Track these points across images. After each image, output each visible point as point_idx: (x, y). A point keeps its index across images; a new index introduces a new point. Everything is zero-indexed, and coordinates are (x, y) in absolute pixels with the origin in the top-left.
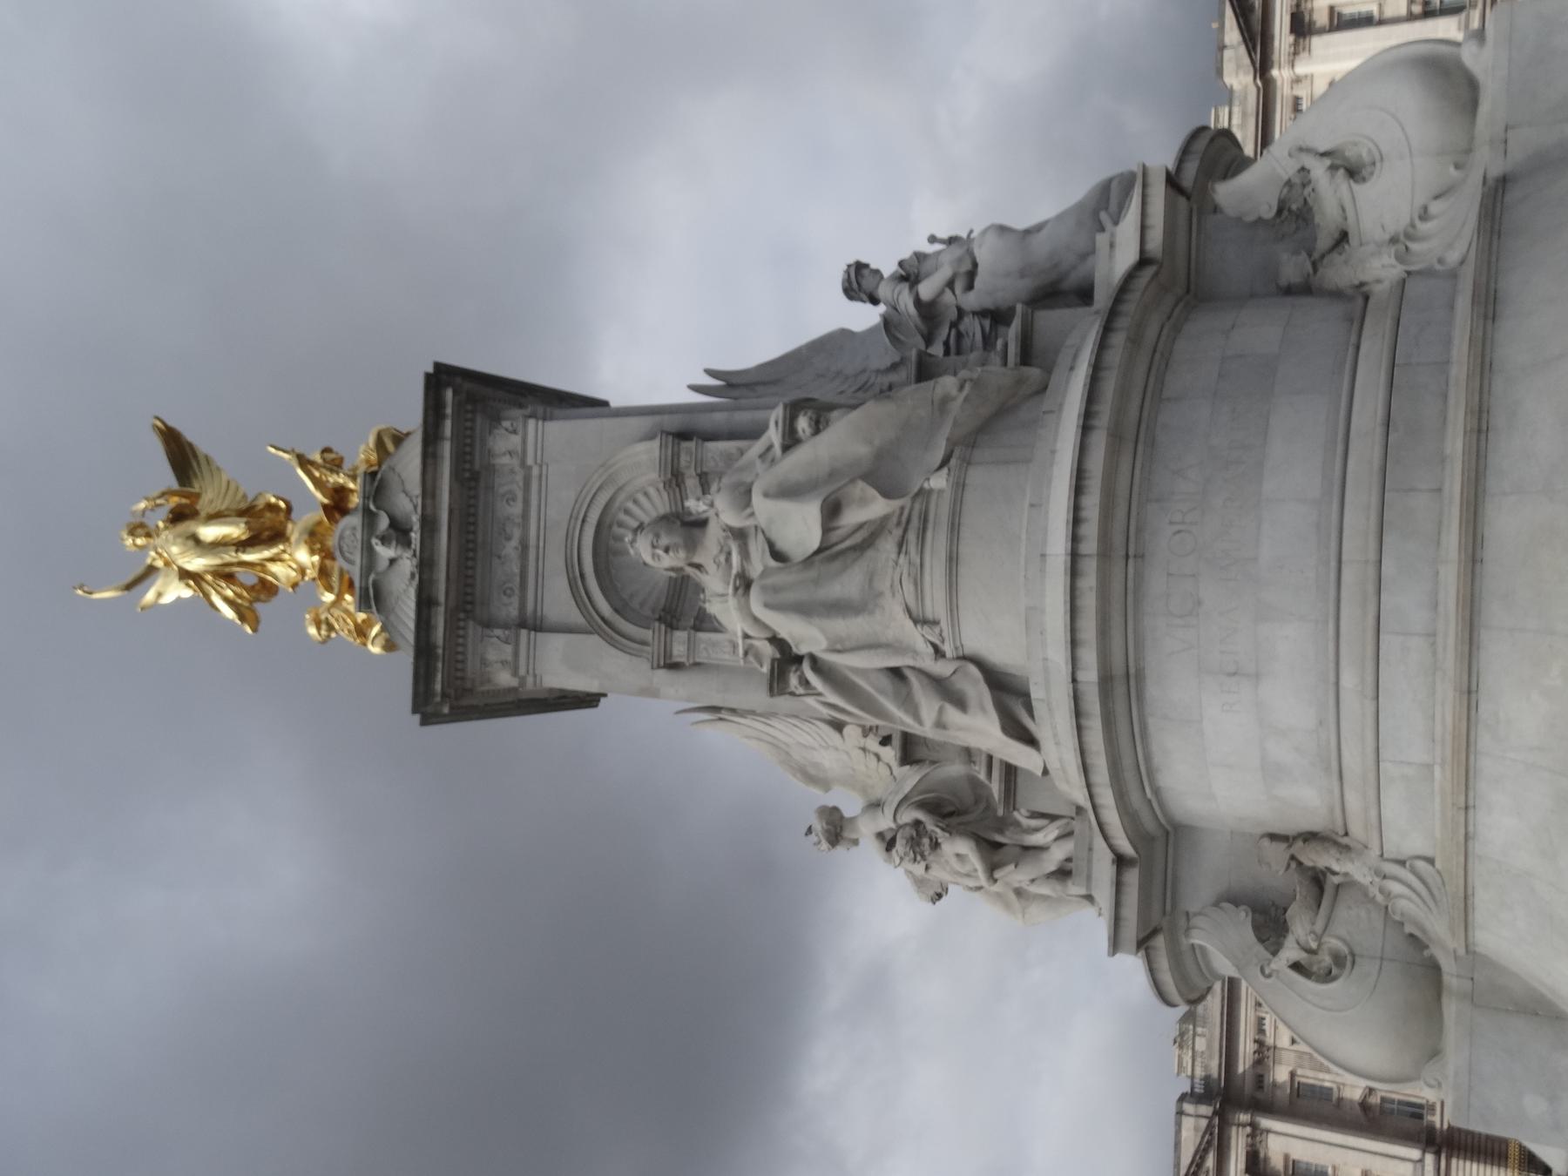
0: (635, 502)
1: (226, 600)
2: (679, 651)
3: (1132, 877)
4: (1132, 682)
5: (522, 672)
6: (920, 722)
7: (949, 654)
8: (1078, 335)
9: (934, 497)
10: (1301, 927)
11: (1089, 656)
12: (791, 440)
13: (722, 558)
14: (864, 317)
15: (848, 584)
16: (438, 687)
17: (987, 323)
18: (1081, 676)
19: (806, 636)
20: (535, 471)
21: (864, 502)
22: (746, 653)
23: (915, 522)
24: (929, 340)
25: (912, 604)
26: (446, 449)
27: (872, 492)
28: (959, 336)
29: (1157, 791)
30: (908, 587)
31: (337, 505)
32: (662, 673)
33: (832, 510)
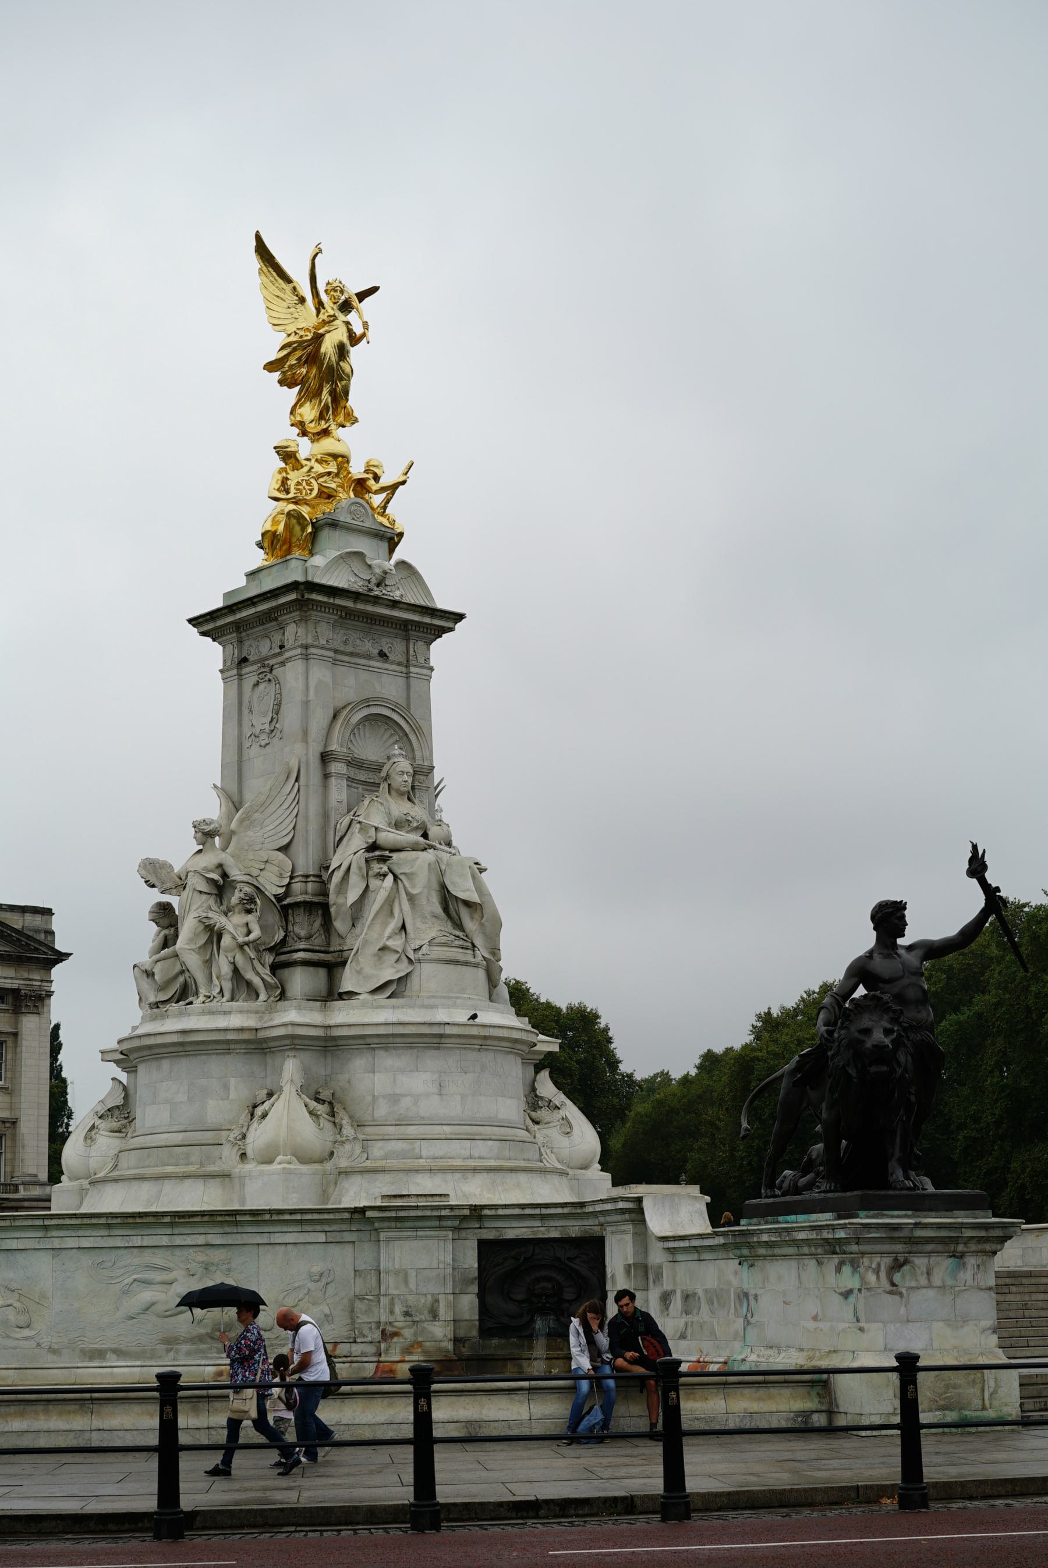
2: (337, 767)
3: (320, 1032)
9: (470, 952)
18: (447, 1026)
20: (404, 670)
23: (466, 944)
25: (436, 941)
26: (427, 620)
29: (374, 1049)
30: (444, 939)
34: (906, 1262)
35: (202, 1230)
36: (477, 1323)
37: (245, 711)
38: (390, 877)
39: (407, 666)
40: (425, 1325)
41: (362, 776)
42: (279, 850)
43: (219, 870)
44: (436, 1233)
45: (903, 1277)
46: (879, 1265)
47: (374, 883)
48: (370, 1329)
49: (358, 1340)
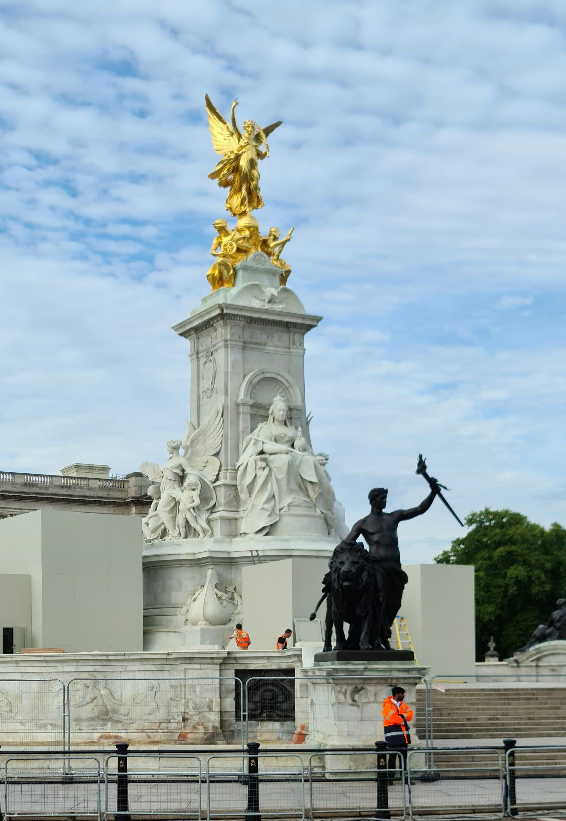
3: (226, 555)
7: (281, 512)
10: (224, 596)
13: (283, 436)
18: (293, 551)
23: (310, 505)
30: (296, 503)
34: (362, 688)
35: (93, 664)
36: (234, 713)
37: (201, 378)
40: (205, 714)
41: (262, 412)
42: (214, 455)
43: (180, 468)
44: (211, 666)
45: (360, 697)
46: (346, 690)
47: (259, 473)
48: (178, 715)
49: (172, 721)
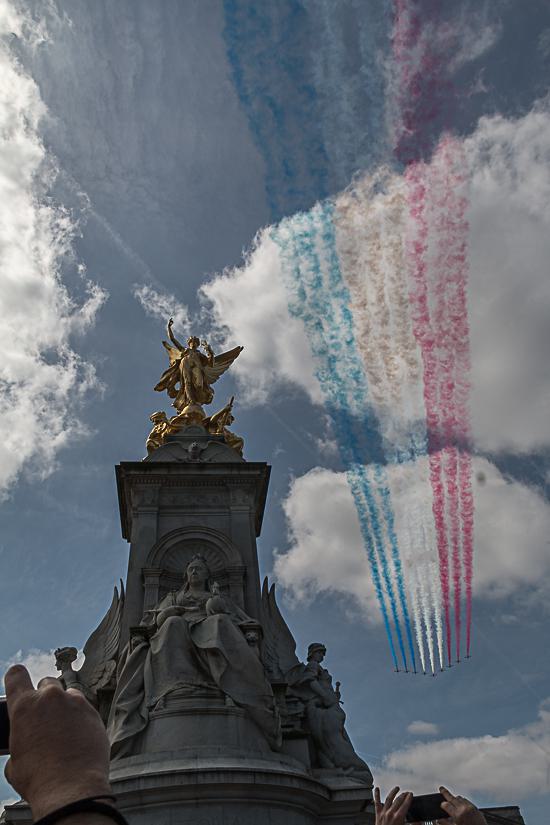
0: (215, 557)
1: (168, 378)
2: (150, 580)
4: (139, 807)
5: (139, 509)
6: (119, 702)
8: (293, 764)
9: (222, 701)
11: (151, 785)
12: (244, 629)
13: (192, 600)
14: (302, 655)
15: (183, 662)
16: (132, 472)
17: (302, 715)
18: (142, 782)
19: (157, 646)
20: (227, 510)
21: (219, 666)
22: (149, 613)
24: (293, 687)
27: (223, 670)
28: (296, 702)
31: (210, 424)
32: (139, 573)
33: (214, 652)
38: (144, 644)
39: (228, 508)
42: (113, 658)
